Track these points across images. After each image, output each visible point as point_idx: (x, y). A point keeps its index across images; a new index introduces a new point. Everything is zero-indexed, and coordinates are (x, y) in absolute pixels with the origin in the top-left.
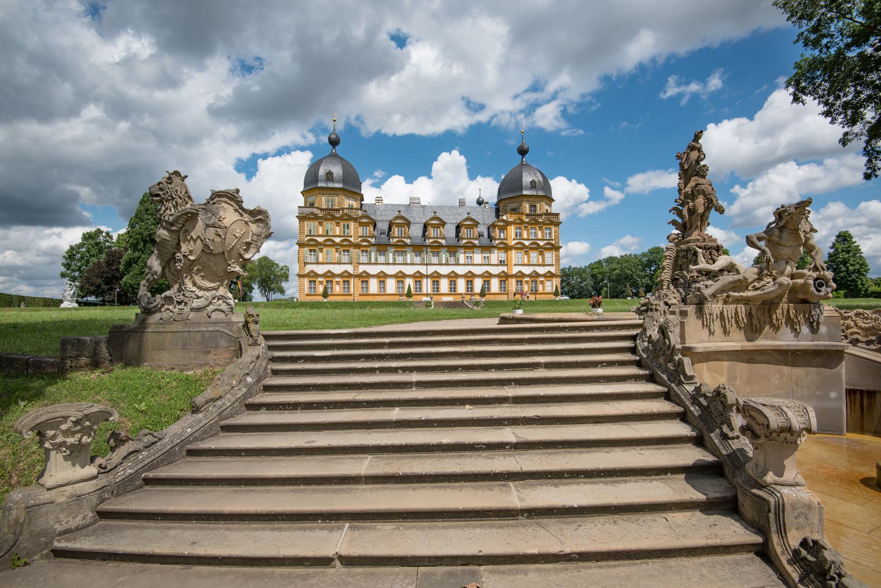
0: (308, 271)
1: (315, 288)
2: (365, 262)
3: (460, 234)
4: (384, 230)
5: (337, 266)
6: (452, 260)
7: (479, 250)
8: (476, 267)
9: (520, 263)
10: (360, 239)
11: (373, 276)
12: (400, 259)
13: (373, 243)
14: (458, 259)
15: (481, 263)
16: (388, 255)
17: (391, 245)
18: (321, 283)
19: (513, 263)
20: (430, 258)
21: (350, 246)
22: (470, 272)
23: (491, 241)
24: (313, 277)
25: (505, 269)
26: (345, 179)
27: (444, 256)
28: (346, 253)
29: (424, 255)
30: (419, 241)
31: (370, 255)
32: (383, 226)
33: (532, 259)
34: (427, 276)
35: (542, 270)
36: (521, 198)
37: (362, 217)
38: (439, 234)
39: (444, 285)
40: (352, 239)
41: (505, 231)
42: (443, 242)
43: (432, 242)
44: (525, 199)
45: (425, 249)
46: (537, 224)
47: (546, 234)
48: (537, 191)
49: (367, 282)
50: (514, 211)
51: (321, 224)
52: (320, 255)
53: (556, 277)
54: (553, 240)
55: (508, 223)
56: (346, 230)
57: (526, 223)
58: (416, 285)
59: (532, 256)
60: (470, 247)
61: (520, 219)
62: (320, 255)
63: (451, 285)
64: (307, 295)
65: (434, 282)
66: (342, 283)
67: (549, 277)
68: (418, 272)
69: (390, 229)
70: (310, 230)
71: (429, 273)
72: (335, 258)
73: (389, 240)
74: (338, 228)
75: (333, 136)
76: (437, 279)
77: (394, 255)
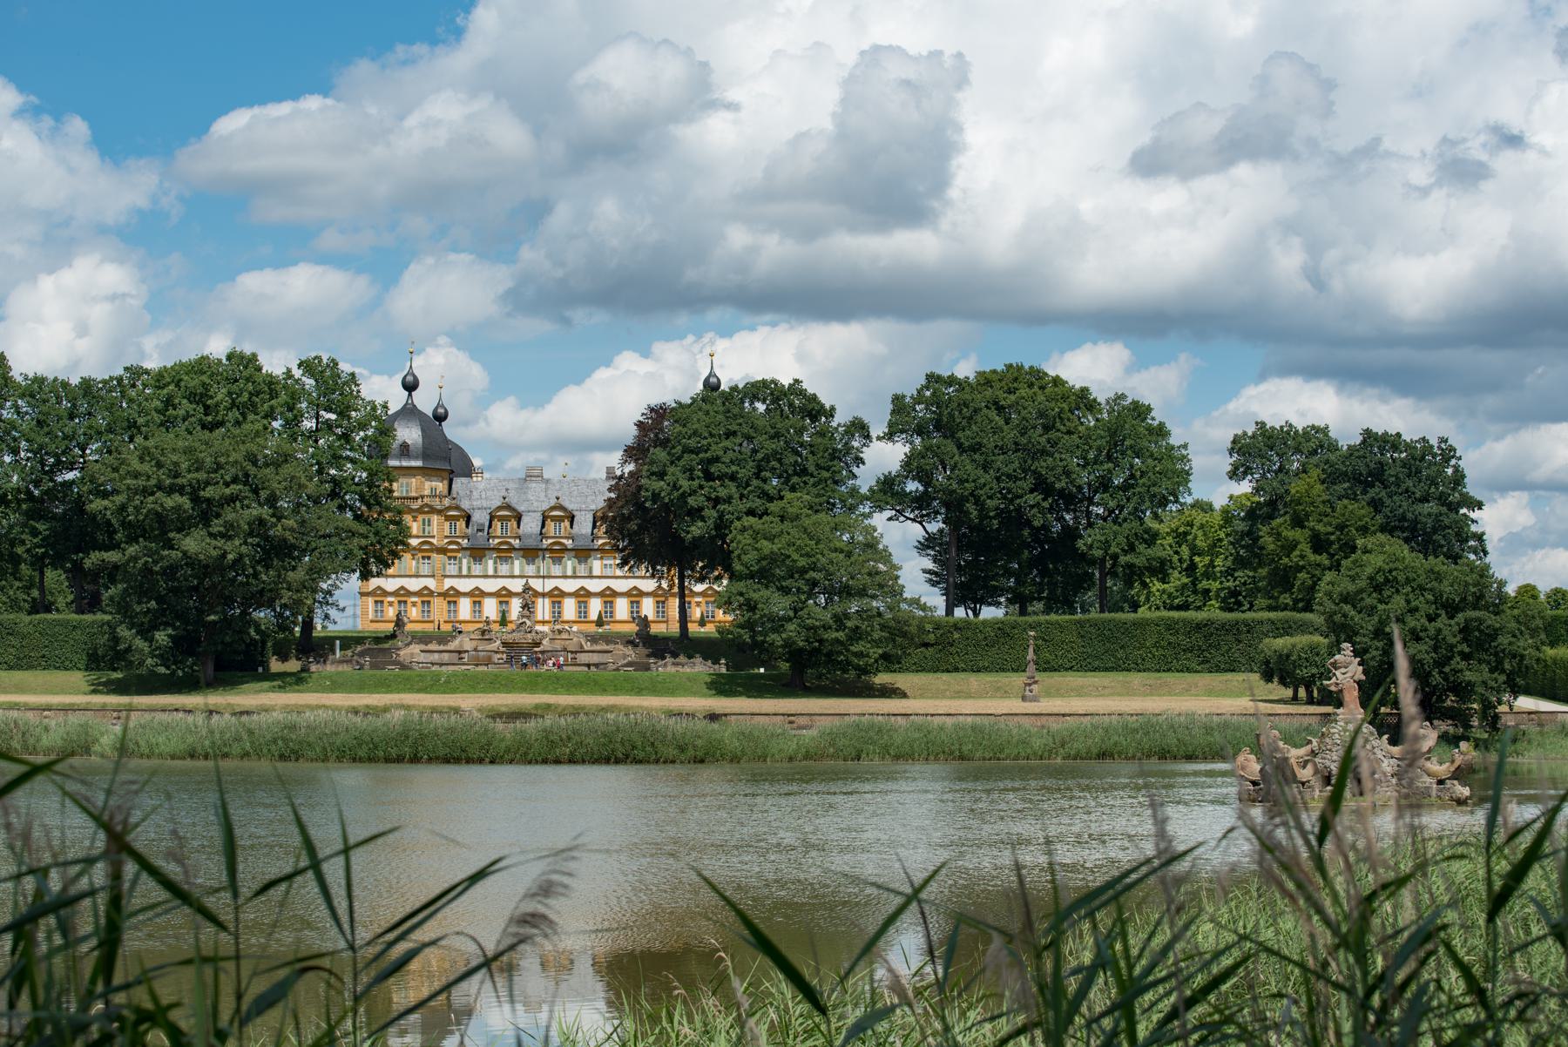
4: (483, 525)
5: (414, 579)
6: (582, 570)
11: (465, 595)
12: (504, 569)
14: (591, 569)
18: (391, 604)
20: (549, 568)
21: (431, 551)
22: (608, 588)
26: (425, 455)
27: (569, 564)
29: (539, 561)
30: (531, 543)
31: (461, 563)
32: (480, 517)
34: (544, 595)
37: (449, 508)
39: (570, 608)
40: (434, 541)
42: (569, 543)
45: (540, 553)
49: (455, 602)
65: (553, 602)
66: (420, 604)
69: (490, 526)
71: (547, 590)
75: (410, 378)
77: (495, 563)
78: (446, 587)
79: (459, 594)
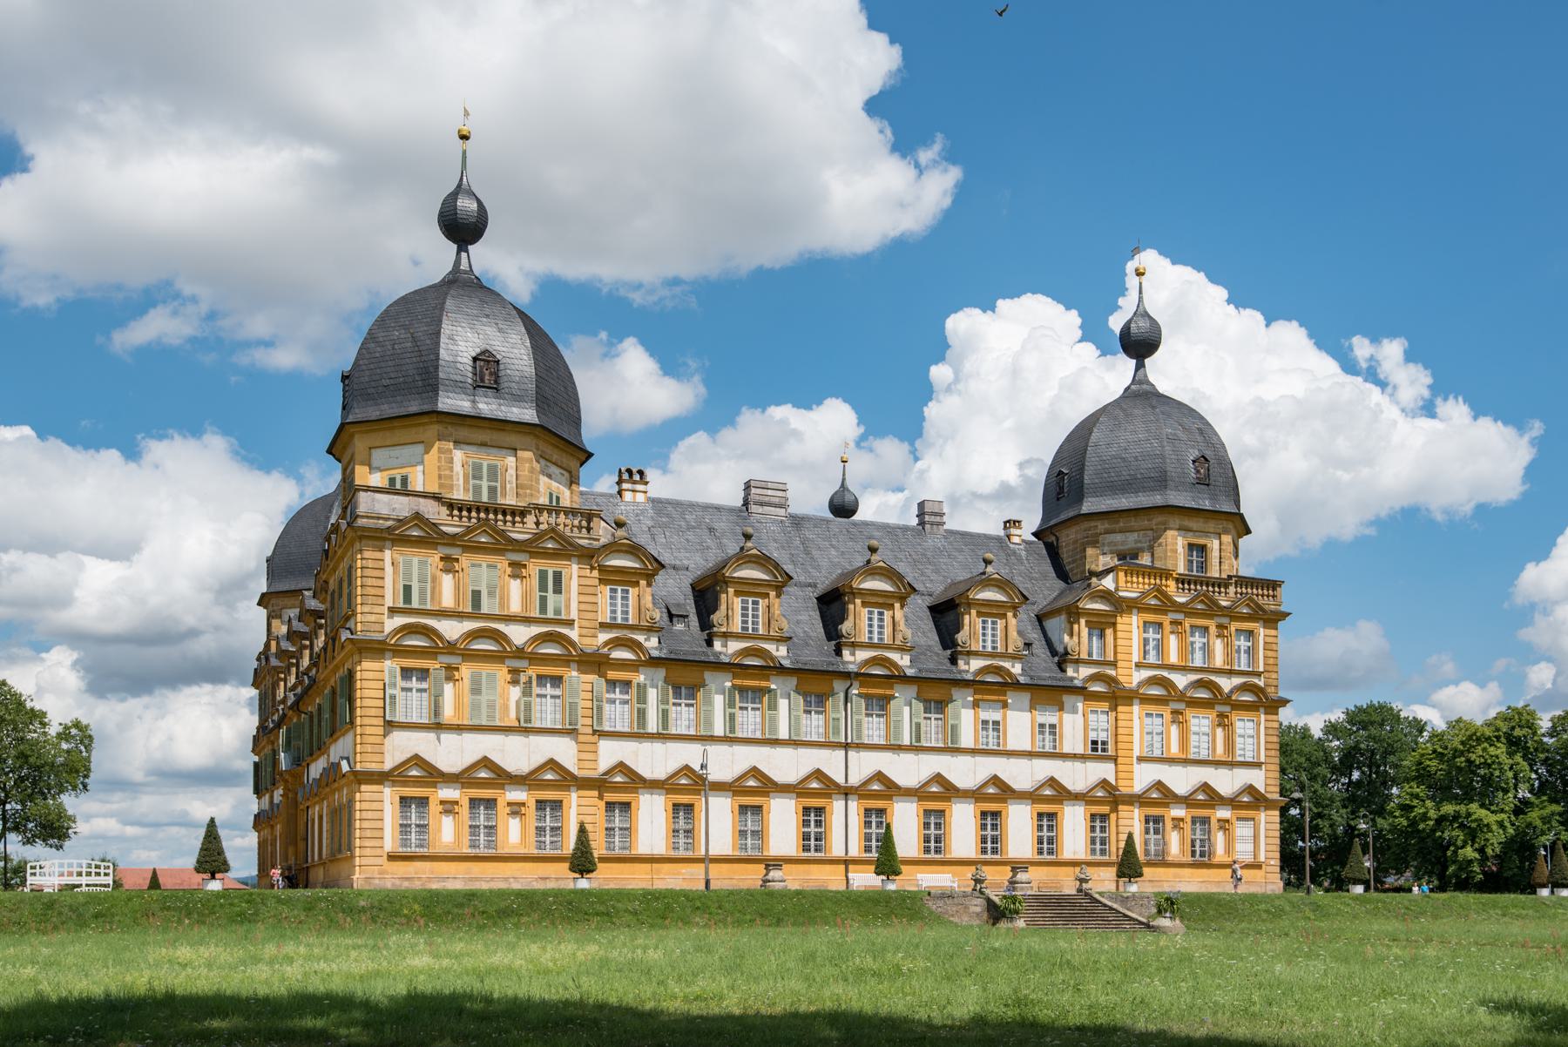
0: (400, 758)
1: (422, 828)
2: (619, 728)
5: (515, 741)
6: (932, 732)
7: (1025, 698)
8: (1013, 761)
9: (1157, 753)
10: (604, 637)
11: (654, 785)
12: (750, 721)
13: (655, 653)
14: (955, 729)
15: (1030, 749)
16: (709, 702)
17: (719, 666)
19: (1136, 753)
20: (859, 723)
21: (564, 661)
23: (1063, 671)
24: (417, 782)
25: (1105, 771)
28: (549, 690)
29: (835, 705)
31: (642, 698)
33: (1193, 739)
34: (846, 792)
35: (1227, 782)
36: (1159, 519)
37: (613, 548)
38: (888, 631)
40: (573, 634)
41: (1109, 632)
42: (903, 660)
43: (868, 662)
44: (1175, 521)
45: (840, 686)
46: (1210, 617)
47: (1238, 651)
48: (1213, 498)
49: (626, 806)
50: (1127, 558)
51: (449, 564)
52: (448, 689)
53: (1267, 808)
54: (1258, 674)
55: (1121, 606)
56: (550, 595)
57: (1179, 608)
58: (806, 823)
59: (1194, 729)
60: (995, 687)
61: (1160, 593)
62: (448, 689)
63: (927, 825)
64: (392, 857)
67: (1247, 806)
68: (818, 774)
70: (407, 590)
71: (854, 780)
72: (506, 707)
73: (709, 643)
74: (515, 587)
76: (879, 804)
77: (731, 704)
78: (604, 764)
79: (636, 782)
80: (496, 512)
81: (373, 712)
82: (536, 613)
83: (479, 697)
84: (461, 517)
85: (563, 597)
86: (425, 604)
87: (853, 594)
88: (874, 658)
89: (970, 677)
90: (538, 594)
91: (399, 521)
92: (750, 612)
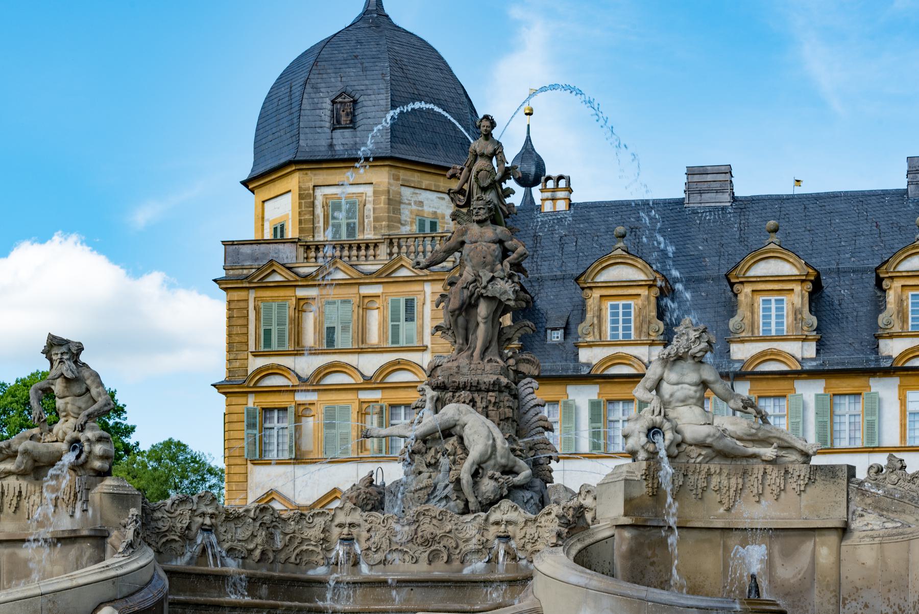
3: (882, 319)
38: (787, 320)
43: (754, 358)
56: (403, 324)
70: (268, 333)
80: (350, 247)
81: (237, 453)
82: (390, 345)
83: (333, 431)
84: (316, 258)
85: (413, 325)
86: (283, 346)
87: (742, 283)
88: (763, 354)
89: (888, 364)
90: (390, 324)
91: (258, 269)
92: (621, 318)
